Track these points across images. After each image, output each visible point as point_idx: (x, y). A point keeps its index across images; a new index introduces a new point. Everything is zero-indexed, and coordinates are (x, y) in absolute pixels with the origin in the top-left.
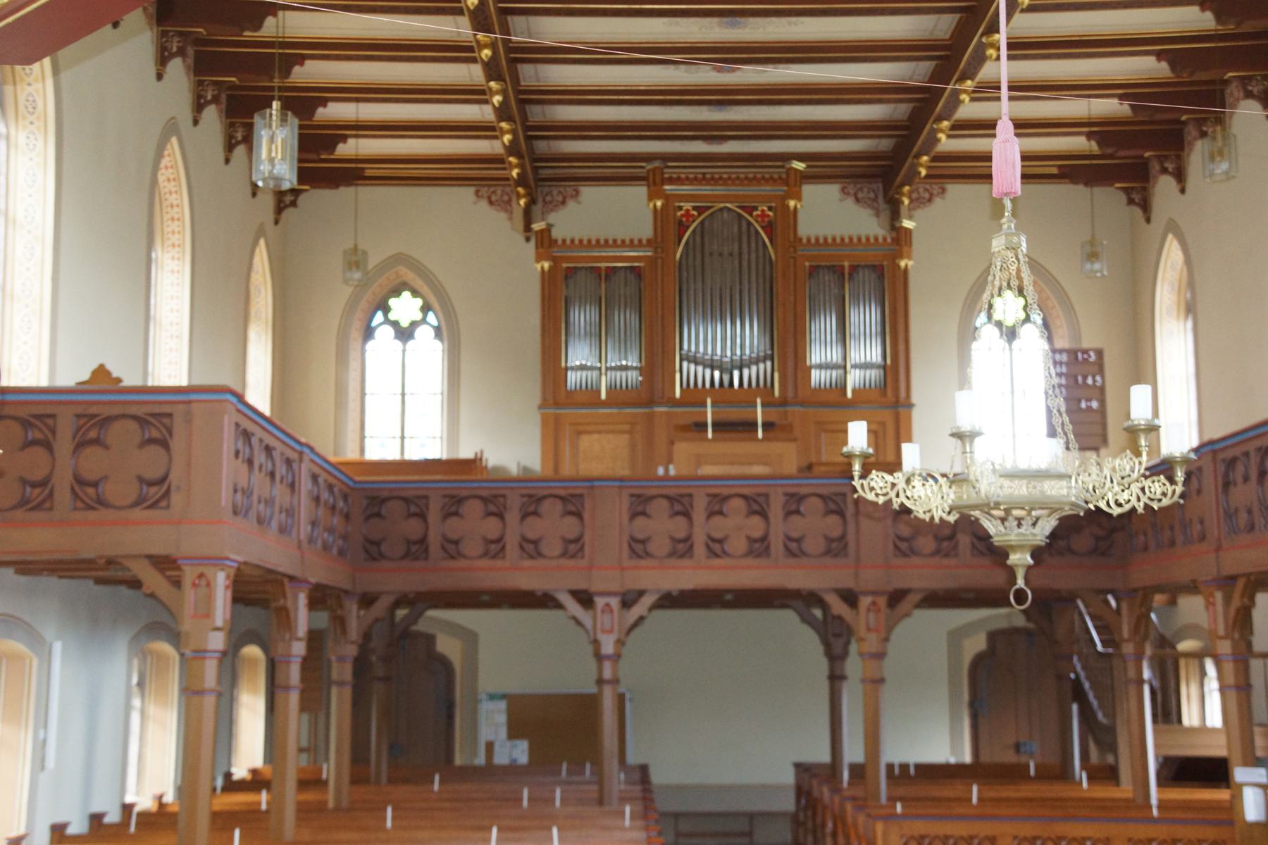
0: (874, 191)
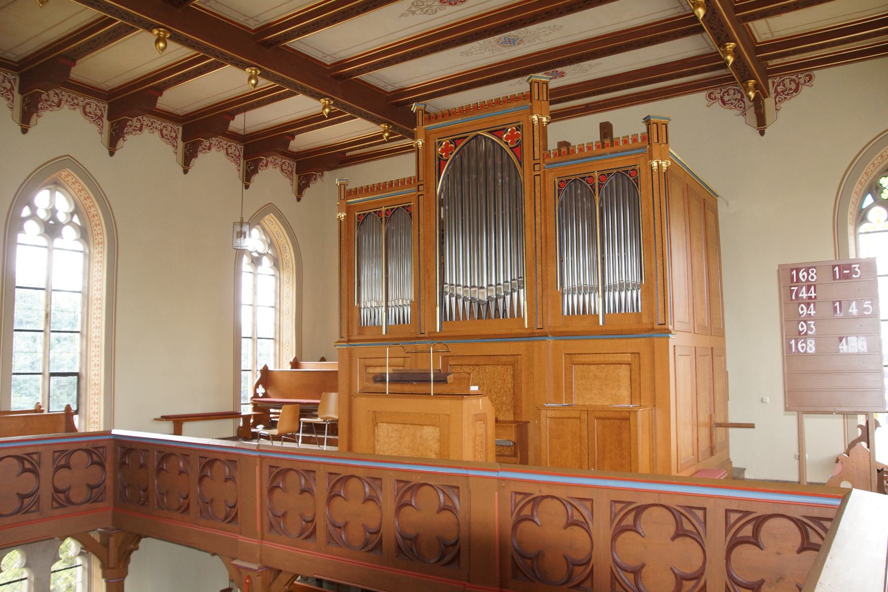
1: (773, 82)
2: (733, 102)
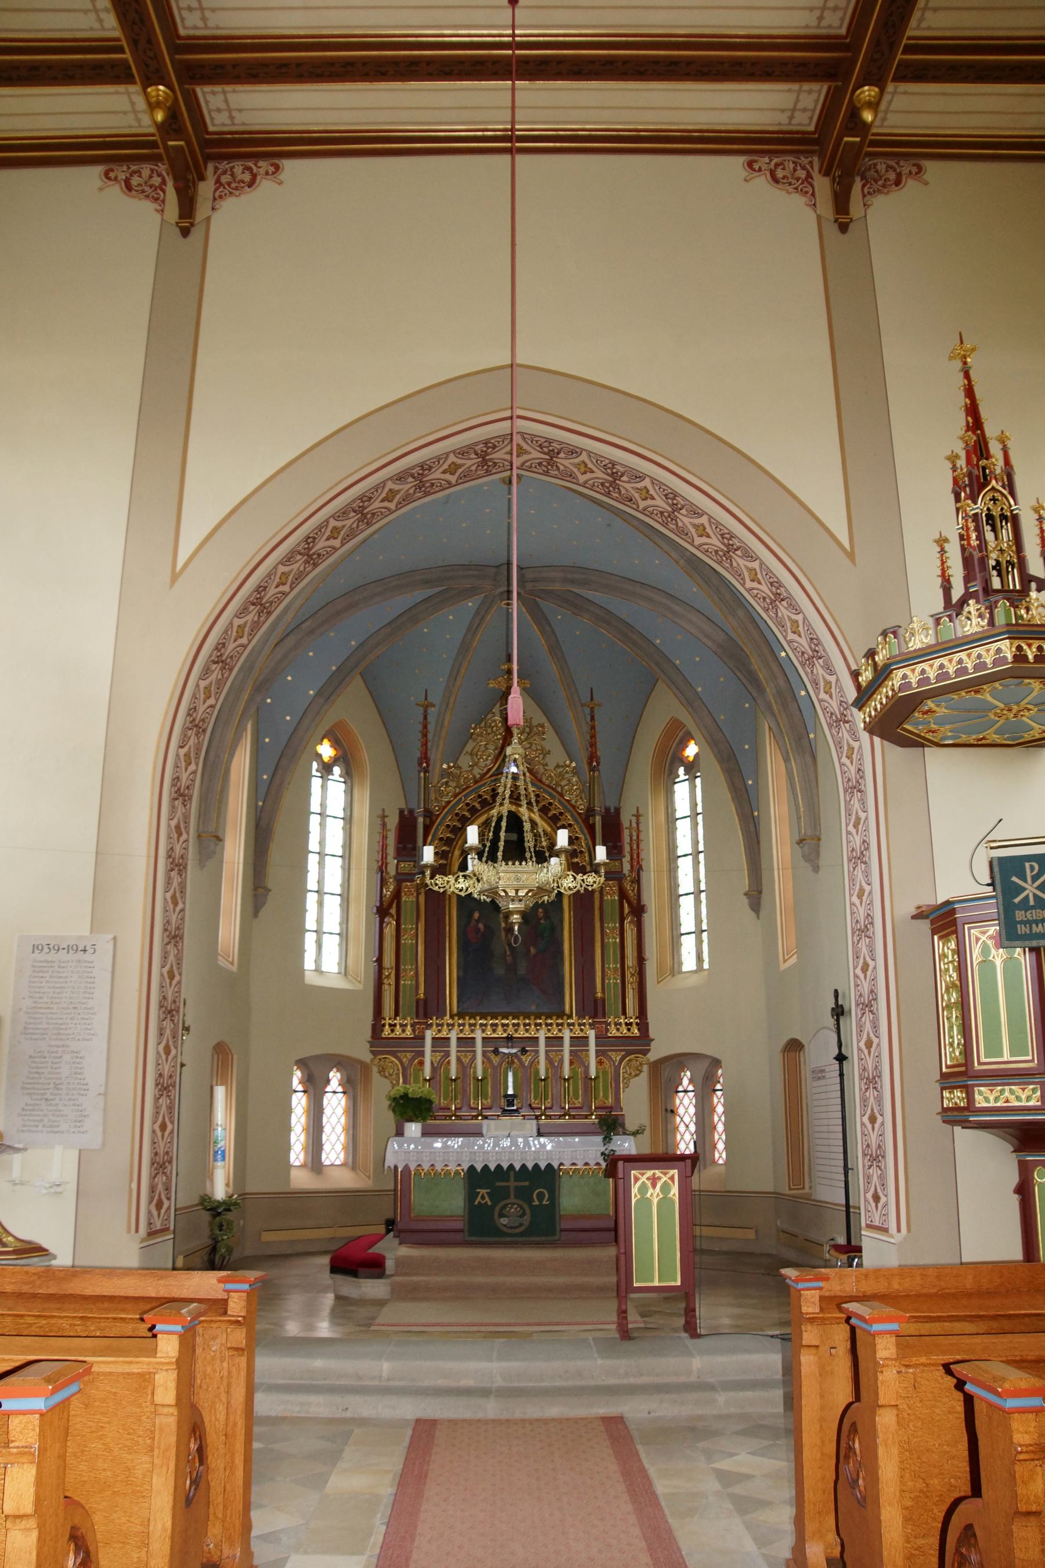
1: (216, 169)
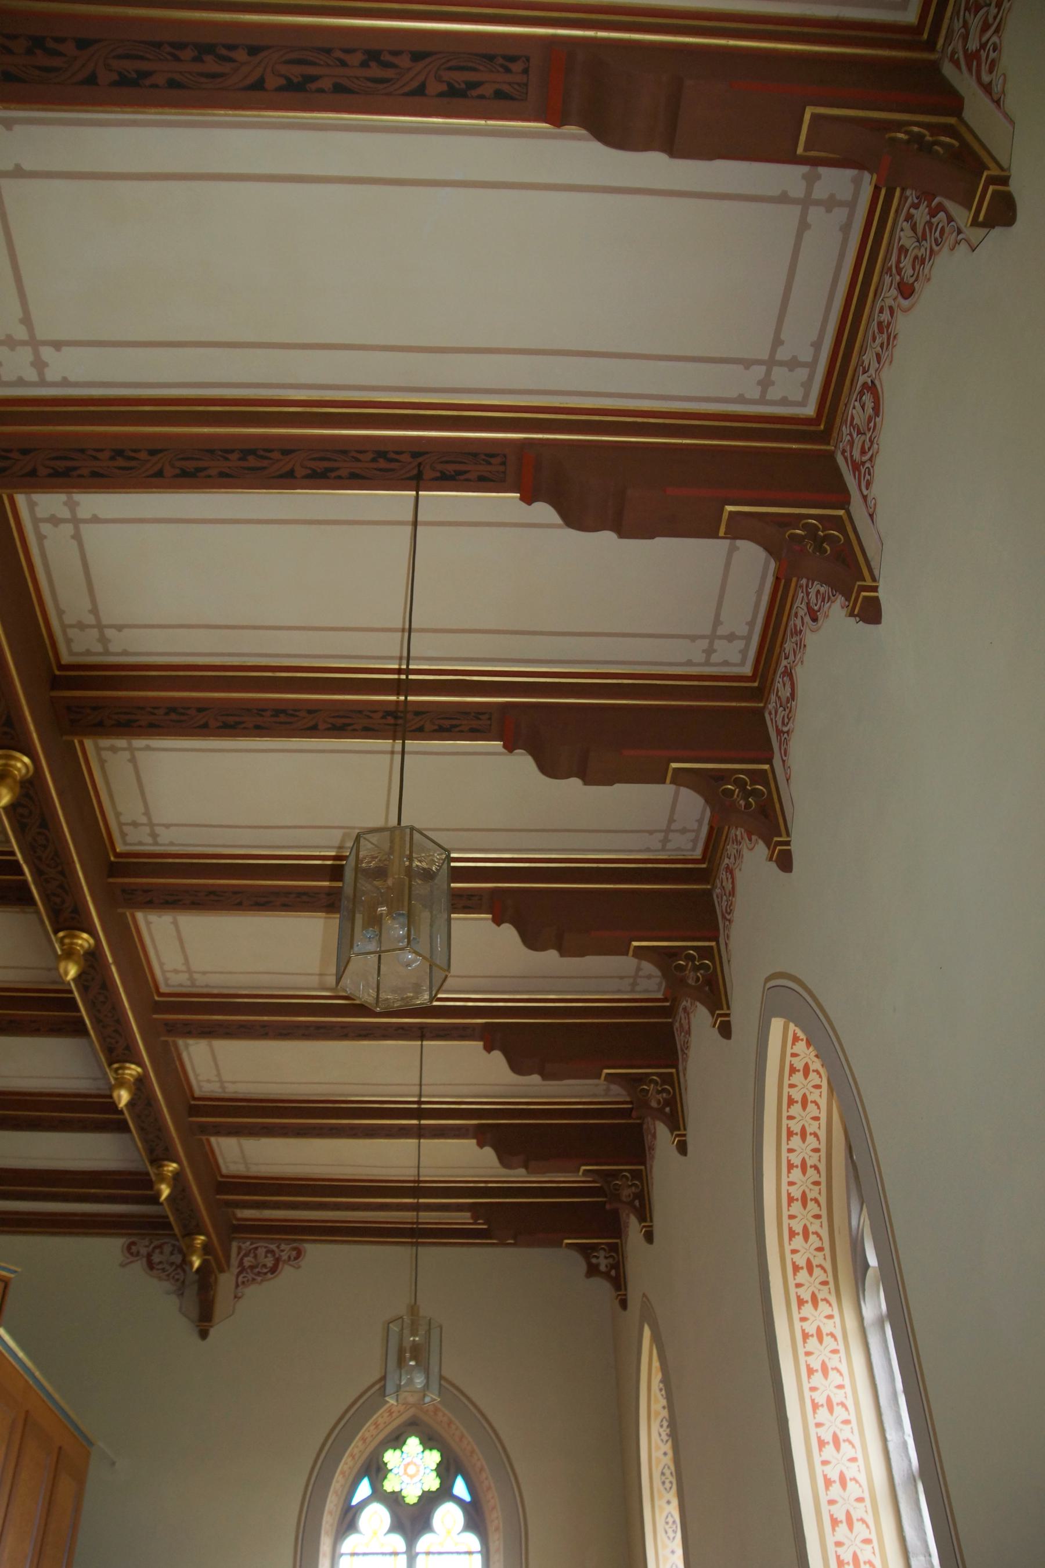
0: (181, 1251)
1: (240, 1248)
2: (167, 1267)
